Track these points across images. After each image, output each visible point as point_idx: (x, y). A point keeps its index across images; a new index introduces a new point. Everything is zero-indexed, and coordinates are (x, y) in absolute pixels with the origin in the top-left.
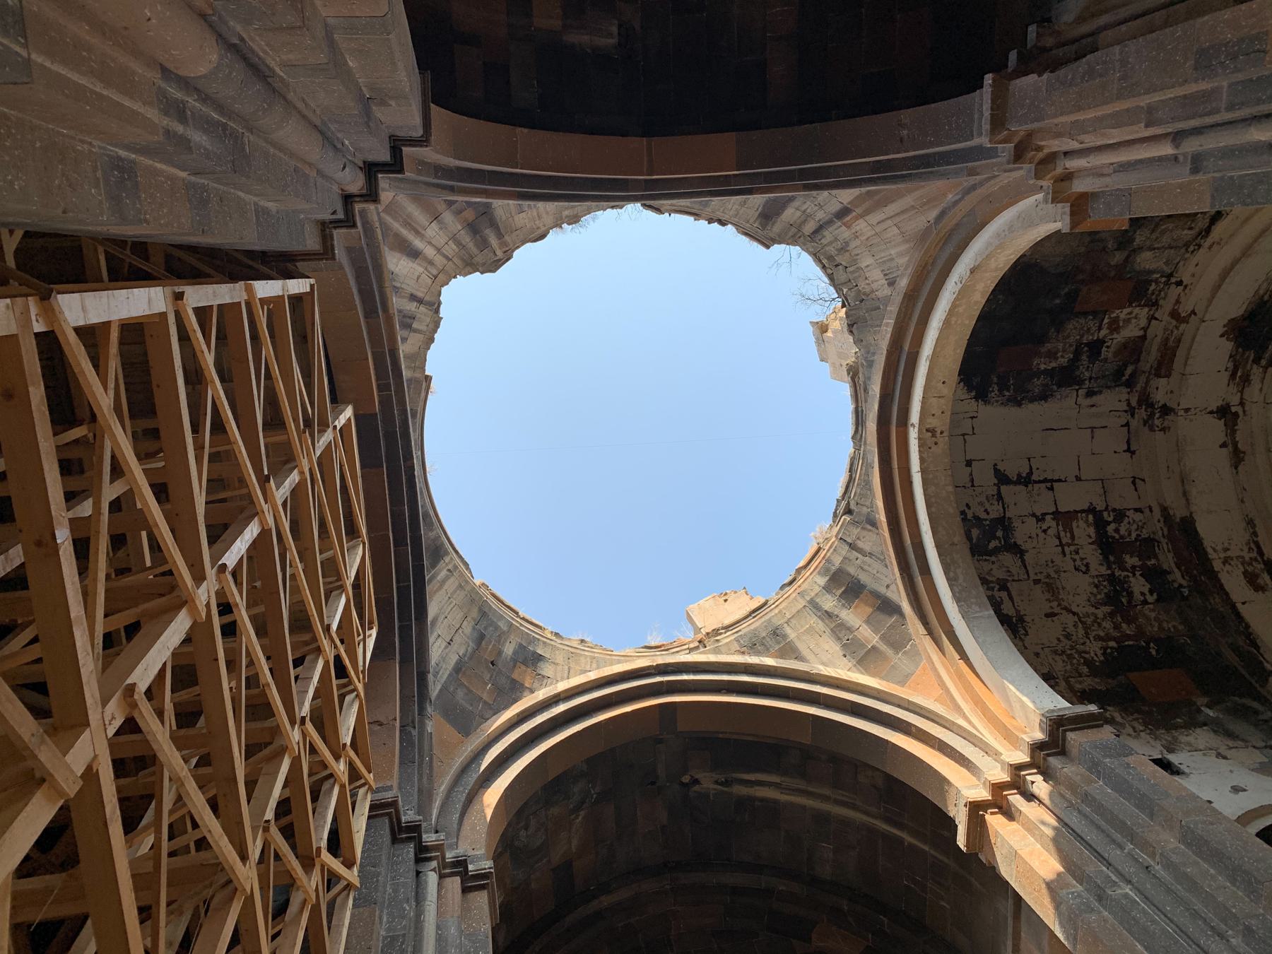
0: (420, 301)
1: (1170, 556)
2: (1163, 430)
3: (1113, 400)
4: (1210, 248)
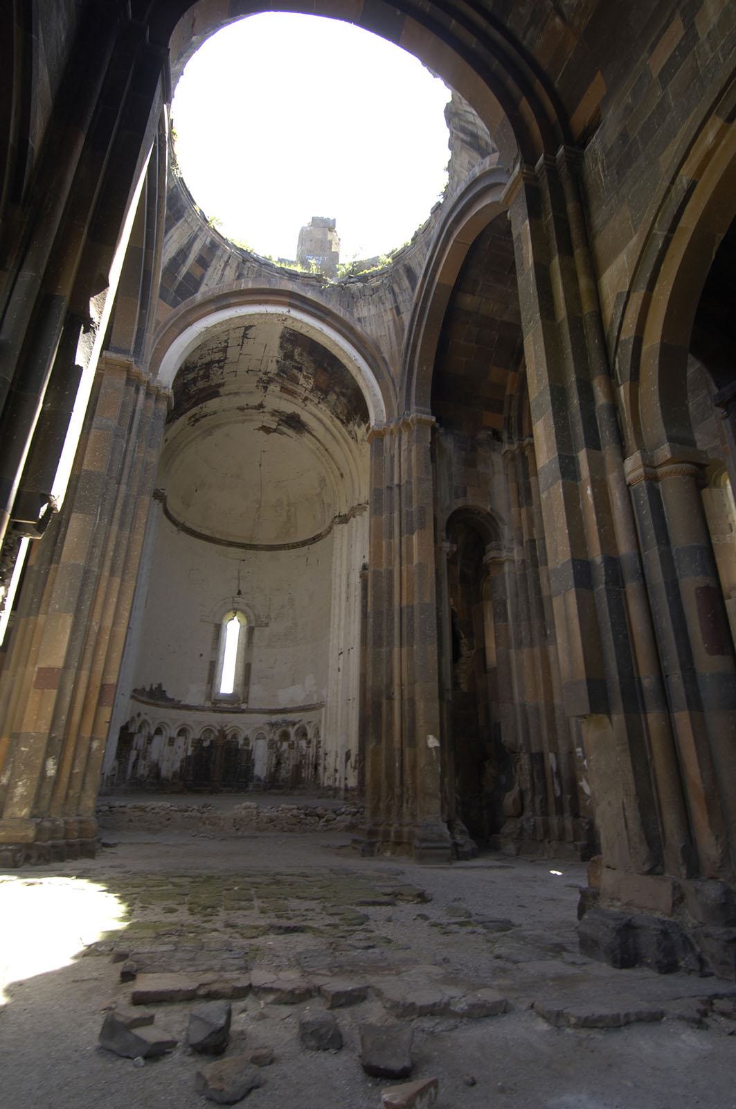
1: (202, 386)
2: (257, 386)
3: (273, 368)
4: (331, 417)
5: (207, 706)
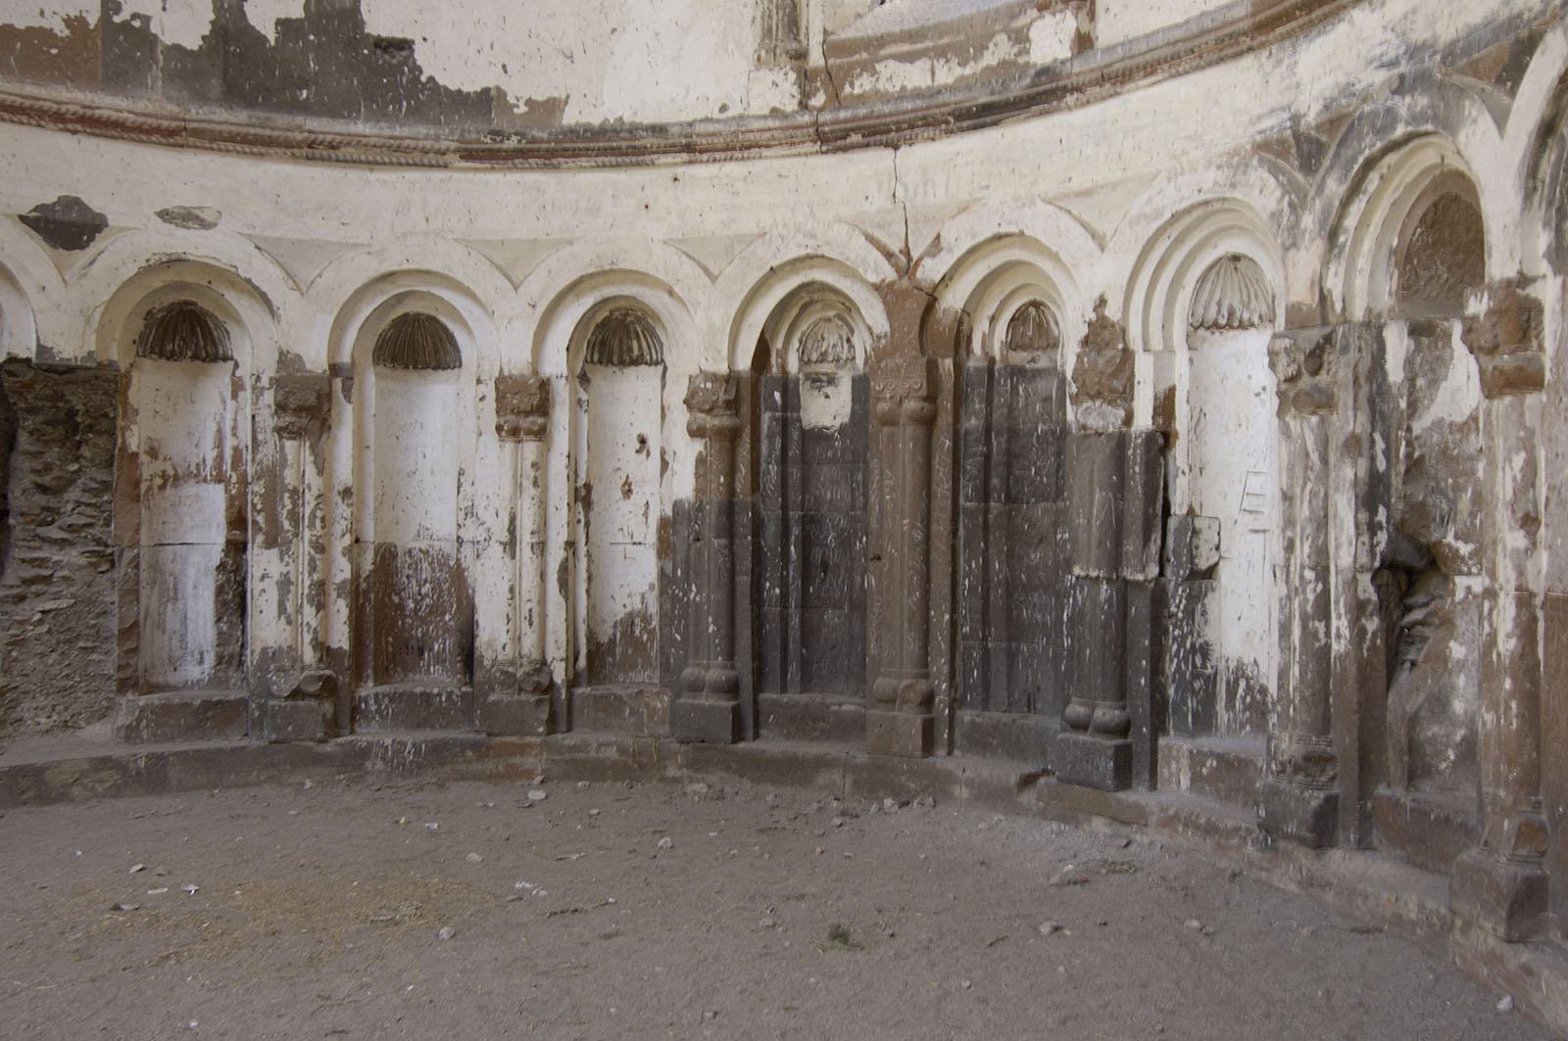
5: (760, 106)
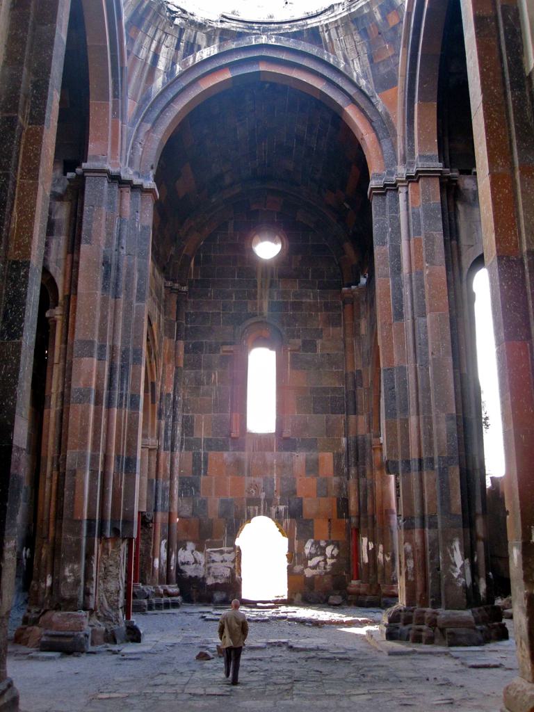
0: (179, 40)
